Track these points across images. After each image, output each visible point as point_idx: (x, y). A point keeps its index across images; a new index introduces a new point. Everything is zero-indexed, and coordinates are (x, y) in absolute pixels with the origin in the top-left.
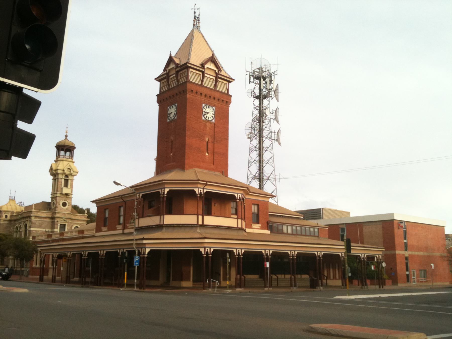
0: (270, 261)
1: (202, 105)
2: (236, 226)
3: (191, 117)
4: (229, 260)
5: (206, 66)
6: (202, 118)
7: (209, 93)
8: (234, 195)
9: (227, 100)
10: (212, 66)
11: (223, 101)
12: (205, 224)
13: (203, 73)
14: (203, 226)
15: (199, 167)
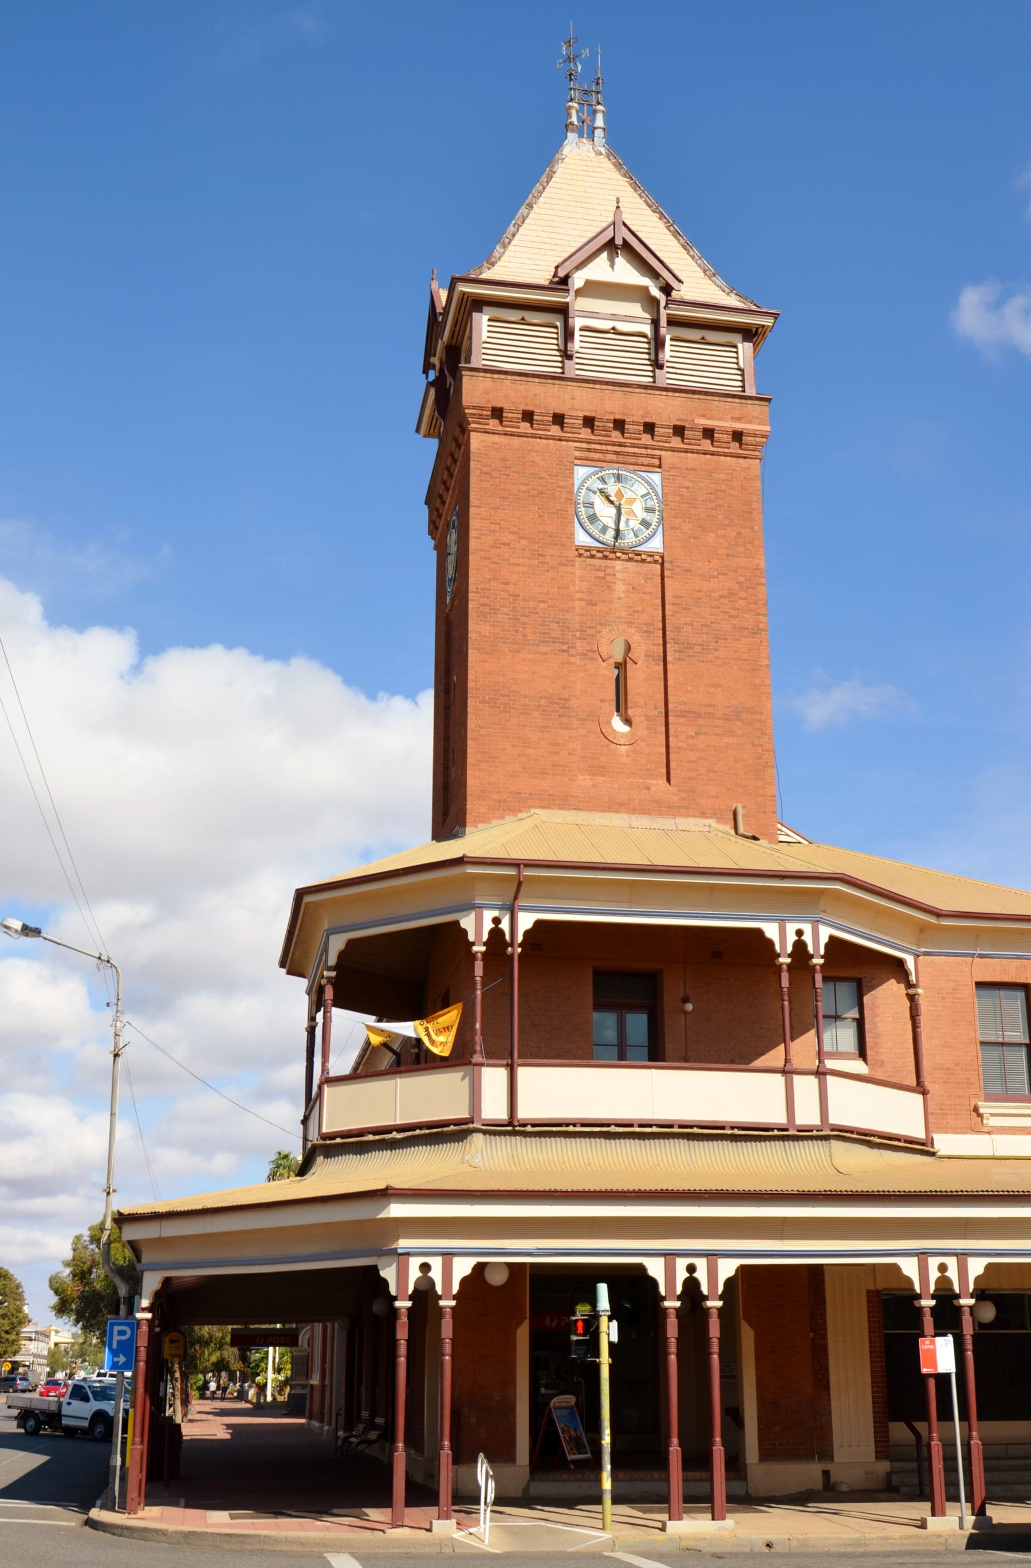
0: (968, 1328)
1: (571, 475)
2: (781, 1119)
3: (497, 545)
4: (610, 1331)
5: (578, 280)
6: (572, 535)
7: (609, 406)
8: (759, 932)
9: (739, 426)
10: (624, 272)
11: (709, 433)
12: (523, 1113)
13: (563, 311)
14: (512, 1127)
15: (563, 801)
